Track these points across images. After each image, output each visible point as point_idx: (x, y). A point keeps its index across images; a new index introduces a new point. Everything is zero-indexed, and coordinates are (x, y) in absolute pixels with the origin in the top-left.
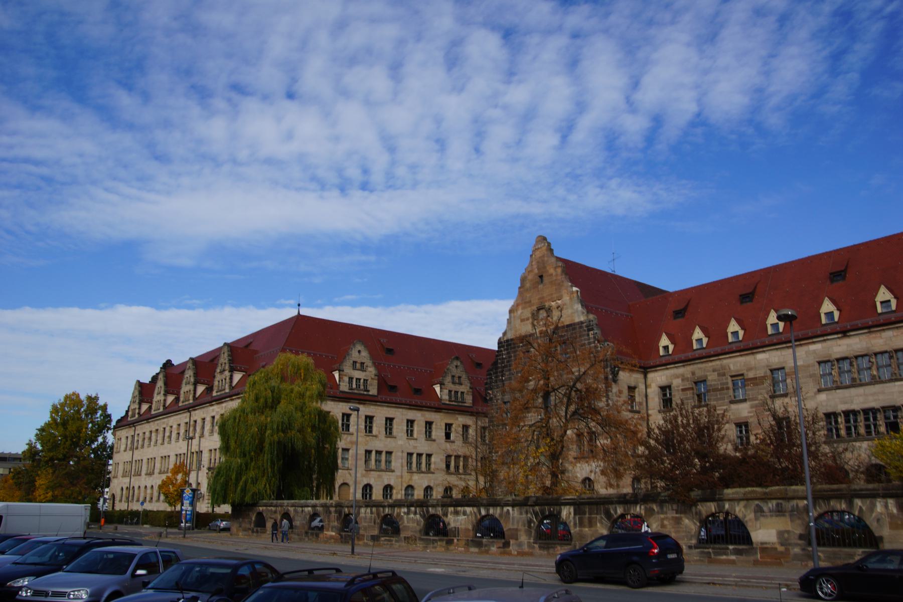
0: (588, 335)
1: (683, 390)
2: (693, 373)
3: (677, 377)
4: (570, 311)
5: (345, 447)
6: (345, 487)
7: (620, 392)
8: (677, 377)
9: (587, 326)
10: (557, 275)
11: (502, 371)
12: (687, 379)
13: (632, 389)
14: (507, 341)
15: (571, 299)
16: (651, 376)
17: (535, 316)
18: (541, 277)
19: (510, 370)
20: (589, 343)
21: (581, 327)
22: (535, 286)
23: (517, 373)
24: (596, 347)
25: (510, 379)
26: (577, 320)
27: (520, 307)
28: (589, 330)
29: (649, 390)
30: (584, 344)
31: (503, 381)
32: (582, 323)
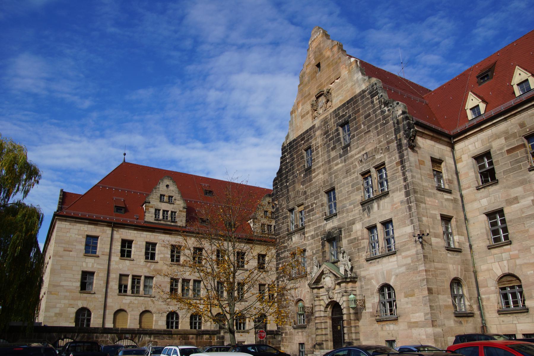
0: (372, 102)
1: (509, 151)
2: (522, 125)
3: (497, 137)
4: (349, 85)
5: (148, 275)
6: (147, 315)
7: (422, 163)
8: (497, 137)
9: (370, 93)
10: (333, 55)
11: (286, 177)
12: (514, 135)
13: (436, 162)
14: (290, 143)
15: (350, 72)
16: (458, 147)
17: (314, 108)
18: (318, 65)
19: (293, 173)
20: (375, 111)
21: (363, 97)
22: (313, 76)
23: (300, 174)
24: (383, 112)
25: (294, 182)
26: (358, 91)
27: (300, 105)
28: (372, 97)
29: (459, 165)
30: (369, 115)
31: (287, 187)
32: (364, 91)
